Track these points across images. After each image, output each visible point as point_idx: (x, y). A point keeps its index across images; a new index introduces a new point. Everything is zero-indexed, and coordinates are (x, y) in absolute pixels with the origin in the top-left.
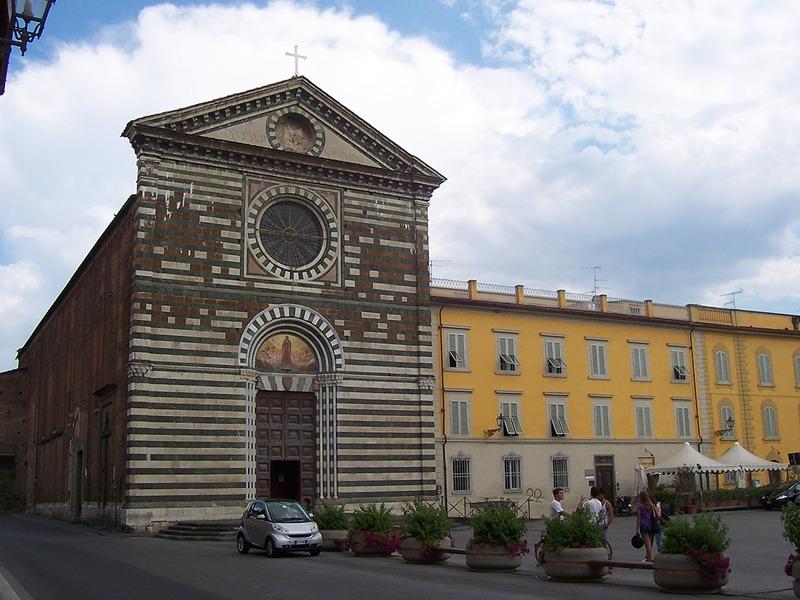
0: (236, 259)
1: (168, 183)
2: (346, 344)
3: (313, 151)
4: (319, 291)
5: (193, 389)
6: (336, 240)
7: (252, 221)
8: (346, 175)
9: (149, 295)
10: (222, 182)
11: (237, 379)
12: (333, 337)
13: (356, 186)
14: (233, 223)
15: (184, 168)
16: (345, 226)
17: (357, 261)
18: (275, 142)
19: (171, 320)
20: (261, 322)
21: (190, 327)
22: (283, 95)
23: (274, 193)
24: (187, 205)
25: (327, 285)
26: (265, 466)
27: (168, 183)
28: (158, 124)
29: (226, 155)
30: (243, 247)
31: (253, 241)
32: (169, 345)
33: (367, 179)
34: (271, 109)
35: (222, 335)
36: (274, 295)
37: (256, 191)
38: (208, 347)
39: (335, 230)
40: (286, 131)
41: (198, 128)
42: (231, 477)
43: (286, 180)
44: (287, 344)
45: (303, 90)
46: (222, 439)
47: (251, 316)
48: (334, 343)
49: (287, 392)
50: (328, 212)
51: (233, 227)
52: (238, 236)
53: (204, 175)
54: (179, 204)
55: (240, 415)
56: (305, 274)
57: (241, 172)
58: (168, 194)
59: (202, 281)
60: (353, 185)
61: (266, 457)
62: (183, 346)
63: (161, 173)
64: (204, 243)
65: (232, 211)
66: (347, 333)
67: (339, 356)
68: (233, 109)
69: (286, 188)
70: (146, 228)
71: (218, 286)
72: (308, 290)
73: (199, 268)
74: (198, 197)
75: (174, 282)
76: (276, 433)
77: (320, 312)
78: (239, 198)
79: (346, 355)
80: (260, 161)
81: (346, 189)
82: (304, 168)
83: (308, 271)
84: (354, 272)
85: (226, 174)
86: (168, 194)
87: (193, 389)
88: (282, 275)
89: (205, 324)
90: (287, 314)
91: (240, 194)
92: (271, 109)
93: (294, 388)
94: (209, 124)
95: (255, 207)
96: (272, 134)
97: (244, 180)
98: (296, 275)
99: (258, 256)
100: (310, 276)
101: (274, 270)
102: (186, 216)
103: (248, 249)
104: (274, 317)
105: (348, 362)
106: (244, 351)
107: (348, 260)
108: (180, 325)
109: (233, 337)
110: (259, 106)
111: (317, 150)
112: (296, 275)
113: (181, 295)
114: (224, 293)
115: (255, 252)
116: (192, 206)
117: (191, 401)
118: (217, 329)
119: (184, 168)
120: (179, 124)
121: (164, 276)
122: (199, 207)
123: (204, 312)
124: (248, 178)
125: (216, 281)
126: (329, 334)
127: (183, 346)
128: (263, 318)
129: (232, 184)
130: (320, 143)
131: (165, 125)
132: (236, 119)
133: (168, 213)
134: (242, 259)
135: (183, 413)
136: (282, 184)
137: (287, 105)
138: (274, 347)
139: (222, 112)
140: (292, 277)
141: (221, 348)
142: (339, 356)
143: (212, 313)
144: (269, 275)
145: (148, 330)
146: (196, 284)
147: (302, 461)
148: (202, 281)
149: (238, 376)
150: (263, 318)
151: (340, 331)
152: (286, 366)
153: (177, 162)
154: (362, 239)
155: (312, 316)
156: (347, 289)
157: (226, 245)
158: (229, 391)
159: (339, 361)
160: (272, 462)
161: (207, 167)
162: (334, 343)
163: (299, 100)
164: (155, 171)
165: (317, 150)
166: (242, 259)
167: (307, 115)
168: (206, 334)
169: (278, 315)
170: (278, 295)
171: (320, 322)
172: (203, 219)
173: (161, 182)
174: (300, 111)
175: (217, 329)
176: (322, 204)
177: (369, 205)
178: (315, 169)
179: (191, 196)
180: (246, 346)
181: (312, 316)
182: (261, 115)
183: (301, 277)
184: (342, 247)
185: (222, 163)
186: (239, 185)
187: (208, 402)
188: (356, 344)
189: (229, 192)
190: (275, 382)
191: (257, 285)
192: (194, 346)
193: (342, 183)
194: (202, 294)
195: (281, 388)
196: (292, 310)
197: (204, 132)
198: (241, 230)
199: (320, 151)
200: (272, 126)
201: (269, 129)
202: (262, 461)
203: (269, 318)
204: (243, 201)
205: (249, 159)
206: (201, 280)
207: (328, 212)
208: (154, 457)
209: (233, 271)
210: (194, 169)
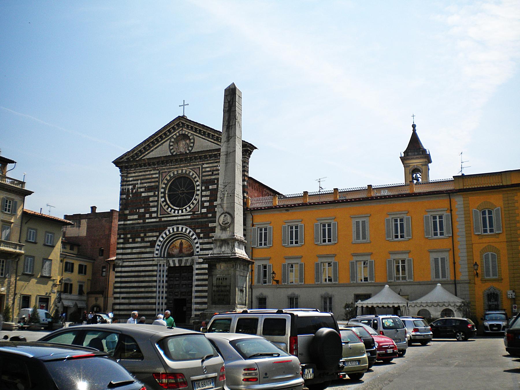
0: (155, 209)
1: (131, 183)
2: (201, 241)
3: (188, 150)
4: (189, 217)
5: (137, 269)
6: (198, 190)
7: (163, 190)
8: (200, 158)
9: (122, 231)
10: (150, 176)
11: (154, 263)
12: (195, 239)
13: (208, 161)
14: (154, 193)
15: (137, 174)
16: (203, 183)
17: (208, 198)
18: (172, 151)
19: (131, 240)
20: (164, 236)
21: (137, 242)
22: (173, 128)
23: (172, 175)
24: (137, 190)
25: (194, 213)
26: (171, 302)
27: (131, 183)
28: (123, 160)
29: (149, 165)
30: (158, 203)
31: (163, 199)
32: (129, 251)
33: (211, 156)
34: (170, 136)
35: (149, 244)
36: (170, 222)
37: (165, 175)
38: (143, 250)
39: (198, 185)
40: (181, 143)
41: (140, 155)
42: (149, 306)
43: (176, 168)
44: (181, 244)
45: (182, 123)
46: (147, 290)
47: (160, 235)
48: (196, 241)
49: (180, 267)
50: (196, 177)
51: (154, 196)
52: (156, 198)
53: (144, 175)
54: (134, 191)
55: (155, 279)
56: (184, 210)
57: (158, 170)
58: (131, 187)
59: (142, 222)
60: (206, 161)
61: (171, 297)
62: (134, 251)
63: (128, 179)
64: (143, 205)
65: (154, 189)
66: (202, 235)
67: (198, 247)
68: (153, 143)
69: (177, 171)
70: (122, 204)
71: (148, 223)
72: (185, 217)
73: (142, 216)
74: (141, 186)
75: (132, 224)
76: (176, 286)
77: (190, 227)
78: (157, 181)
79: (200, 247)
80: (163, 163)
81: (203, 164)
82: (181, 160)
83: (186, 208)
84: (206, 204)
85: (152, 172)
86: (131, 187)
87: (137, 269)
88: (174, 212)
89: (143, 241)
90: (175, 230)
91: (157, 179)
92: (170, 136)
93: (183, 265)
94: (145, 152)
95: (164, 184)
96: (171, 147)
97: (159, 173)
98: (180, 211)
99: (165, 206)
100: (186, 210)
101: (171, 211)
102: (137, 194)
103: (161, 204)
104: (170, 233)
105: (201, 250)
106: (157, 250)
107: (203, 199)
108: (134, 242)
109: (153, 244)
110: (164, 137)
111: (190, 148)
112: (180, 211)
113: (134, 229)
114: (149, 226)
115: (163, 204)
116: (139, 190)
117: (136, 274)
118: (147, 242)
119: (137, 174)
120: (132, 157)
121: (129, 222)
122: (142, 190)
123: (142, 235)
124: (161, 171)
125: (147, 221)
126: (194, 237)
127: (134, 251)
128: (166, 234)
129: (154, 176)
130: (192, 145)
131: (127, 159)
132: (156, 146)
133: (131, 195)
134: (158, 209)
135: (133, 279)
136: (175, 170)
137: (177, 131)
138: (175, 246)
139: (148, 145)
140: (178, 213)
141: (148, 250)
142: (198, 247)
143: (145, 235)
144: (169, 214)
145: (121, 246)
146: (139, 223)
147: (187, 299)
148: (142, 222)
149: (154, 262)
150: (166, 234)
151: (198, 234)
152: (181, 254)
153: (134, 173)
154: (210, 187)
155: (186, 229)
156: (202, 213)
157: (151, 204)
158: (150, 268)
159: (198, 250)
160: (174, 299)
161: (145, 171)
162: (196, 241)
163: (182, 127)
164: (125, 179)
165: (190, 148)
166: (158, 209)
167: (187, 133)
168: (143, 245)
169: (171, 231)
170: (172, 222)
171: (190, 232)
172: (143, 195)
173: (128, 183)
174: (184, 132)
175: (147, 242)
176: (193, 174)
177: (215, 168)
178: (186, 159)
179: (139, 186)
180: (158, 248)
181: (186, 229)
182: (167, 141)
183: (182, 212)
184: (201, 193)
185: (150, 168)
186: (157, 175)
187: (143, 274)
188: (206, 240)
189: (153, 180)
190: (175, 262)
191: (163, 219)
192: (138, 250)
193: (201, 162)
194: (142, 227)
195: (177, 265)
196: (178, 228)
197: (144, 156)
198: (158, 196)
199: (192, 149)
200: (171, 144)
201: (170, 146)
202: (171, 299)
203: (168, 233)
204: (159, 182)
205: (158, 163)
206: (141, 221)
207: (196, 177)
208: (123, 298)
209: (154, 215)
210: (140, 174)
